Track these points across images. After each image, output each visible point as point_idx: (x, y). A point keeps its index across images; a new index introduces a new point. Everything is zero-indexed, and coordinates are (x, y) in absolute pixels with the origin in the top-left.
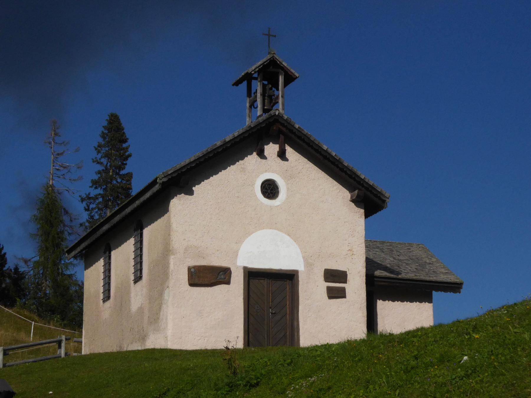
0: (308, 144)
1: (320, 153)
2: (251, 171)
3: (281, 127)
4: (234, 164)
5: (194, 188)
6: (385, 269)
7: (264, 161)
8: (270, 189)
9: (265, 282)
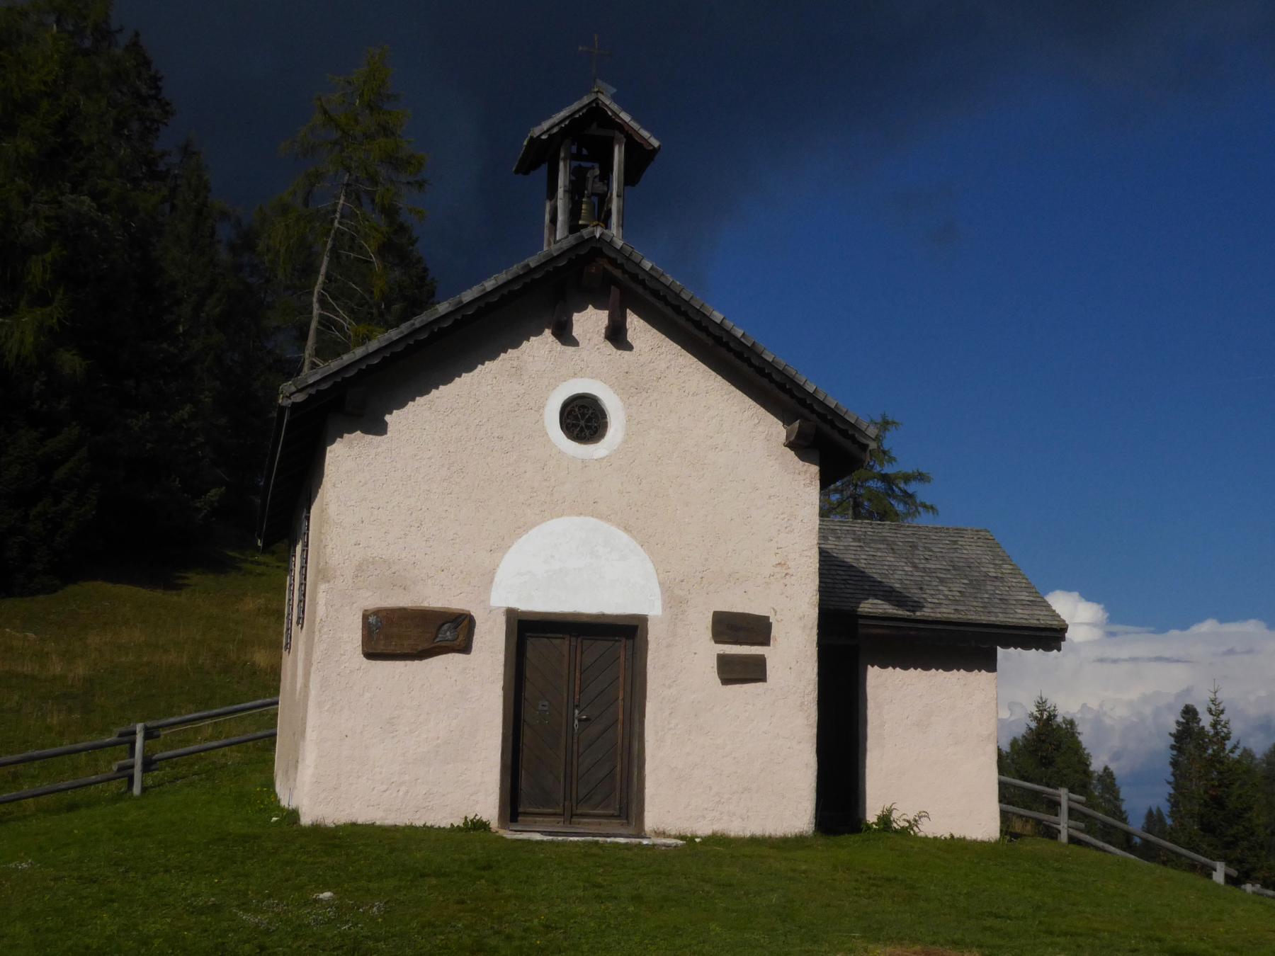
0: (677, 309)
1: (705, 329)
2: (538, 372)
3: (609, 268)
4: (493, 357)
5: (388, 418)
6: (890, 595)
7: (570, 350)
8: (583, 419)
9: (562, 645)
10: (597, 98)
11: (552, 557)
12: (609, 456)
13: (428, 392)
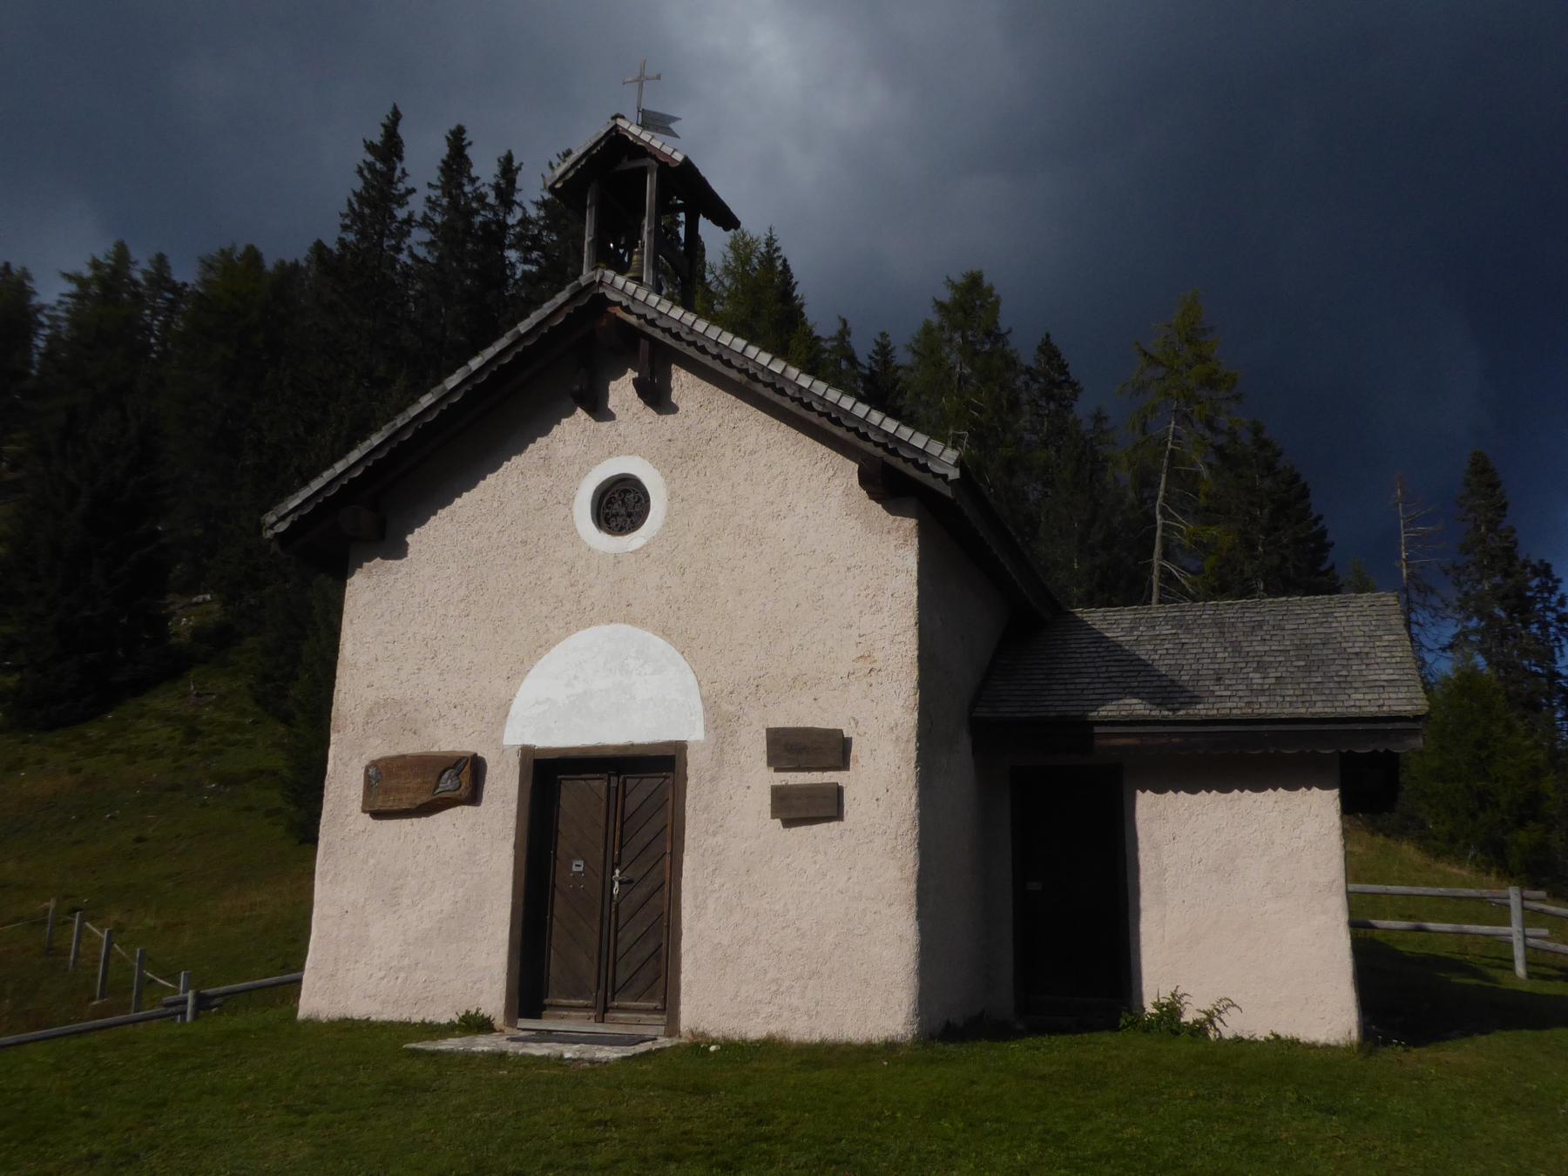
4: (520, 450)
5: (409, 539)
10: (616, 126)
11: (576, 677)
12: (648, 545)
13: (450, 502)
